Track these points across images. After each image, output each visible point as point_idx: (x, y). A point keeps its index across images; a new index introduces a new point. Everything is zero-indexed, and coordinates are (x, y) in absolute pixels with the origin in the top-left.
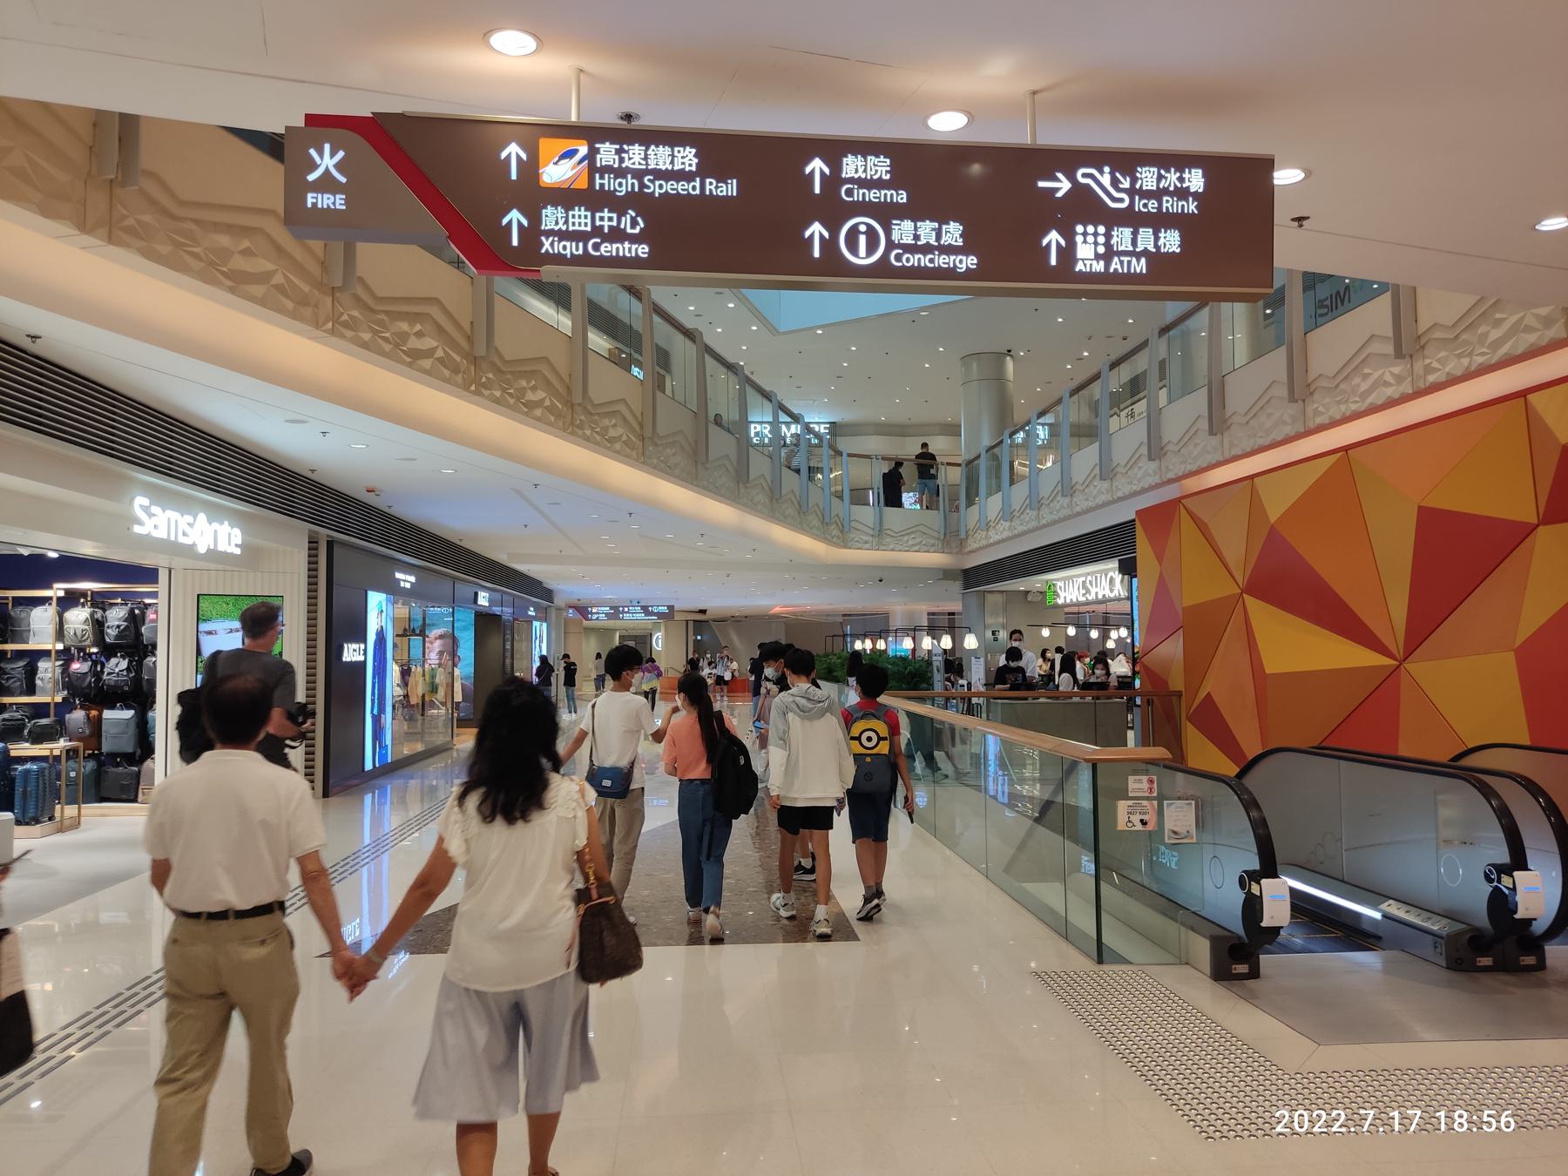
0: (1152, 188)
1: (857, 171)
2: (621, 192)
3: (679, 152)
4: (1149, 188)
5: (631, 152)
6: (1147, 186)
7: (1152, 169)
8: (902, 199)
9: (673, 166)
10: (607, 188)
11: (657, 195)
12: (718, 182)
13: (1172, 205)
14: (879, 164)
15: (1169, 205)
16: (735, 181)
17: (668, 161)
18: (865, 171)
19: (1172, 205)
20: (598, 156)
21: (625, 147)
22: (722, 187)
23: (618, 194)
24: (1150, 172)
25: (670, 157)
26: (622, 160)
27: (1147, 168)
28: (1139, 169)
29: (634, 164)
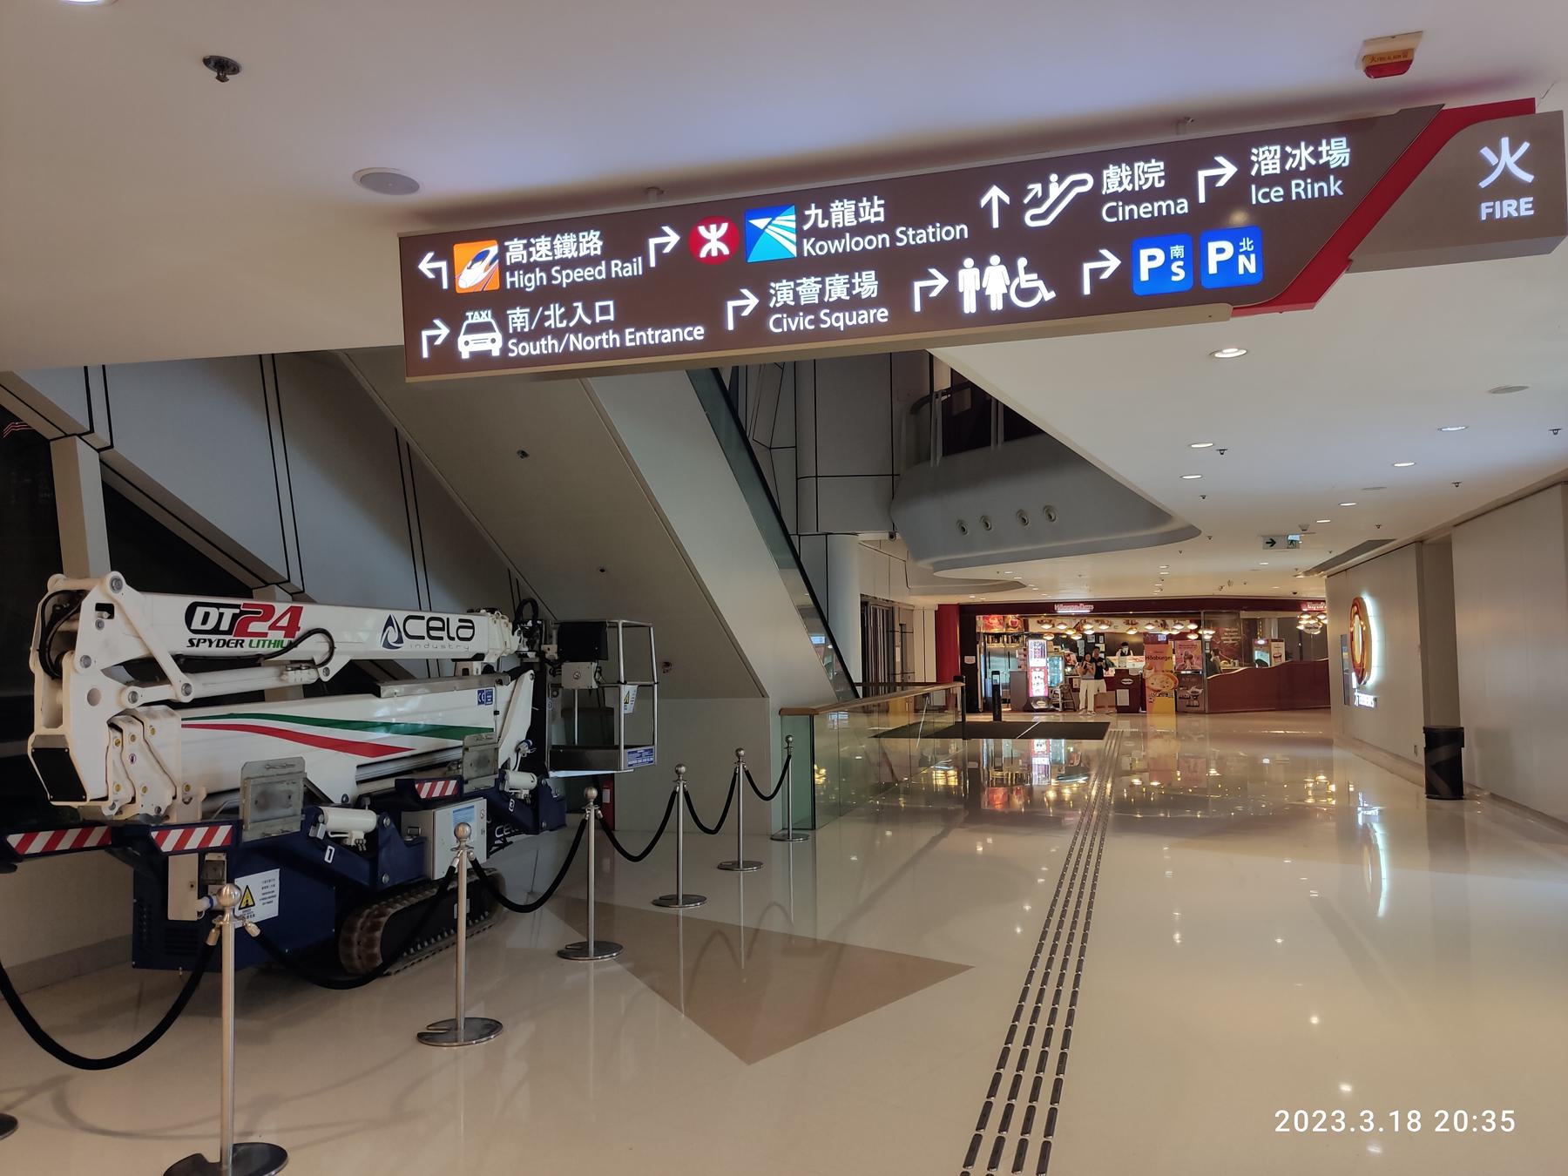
0: (1274, 172)
1: (1121, 183)
2: (530, 287)
3: (584, 237)
4: (1271, 172)
5: (538, 245)
6: (1266, 170)
7: (1272, 148)
8: (1182, 209)
9: (579, 252)
10: (517, 286)
11: (564, 286)
12: (623, 263)
13: (1305, 190)
14: (1150, 170)
15: (1300, 190)
16: (640, 259)
17: (574, 249)
18: (1132, 181)
19: (1305, 190)
20: (508, 254)
21: (532, 241)
22: (627, 267)
23: (527, 289)
24: (1270, 151)
25: (576, 244)
26: (530, 254)
27: (1266, 148)
28: (1254, 151)
29: (541, 256)
